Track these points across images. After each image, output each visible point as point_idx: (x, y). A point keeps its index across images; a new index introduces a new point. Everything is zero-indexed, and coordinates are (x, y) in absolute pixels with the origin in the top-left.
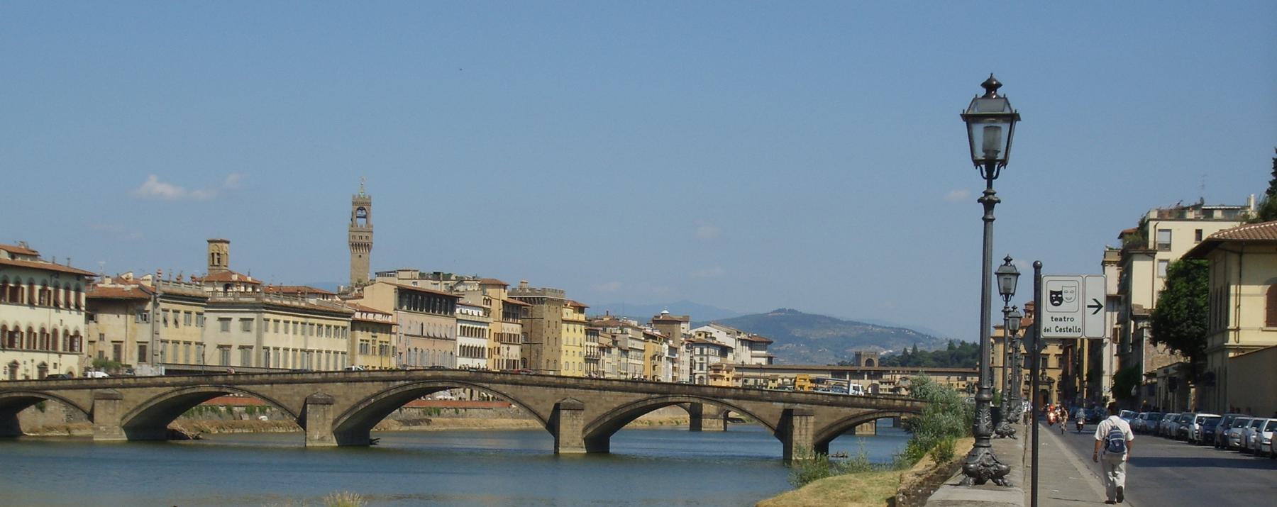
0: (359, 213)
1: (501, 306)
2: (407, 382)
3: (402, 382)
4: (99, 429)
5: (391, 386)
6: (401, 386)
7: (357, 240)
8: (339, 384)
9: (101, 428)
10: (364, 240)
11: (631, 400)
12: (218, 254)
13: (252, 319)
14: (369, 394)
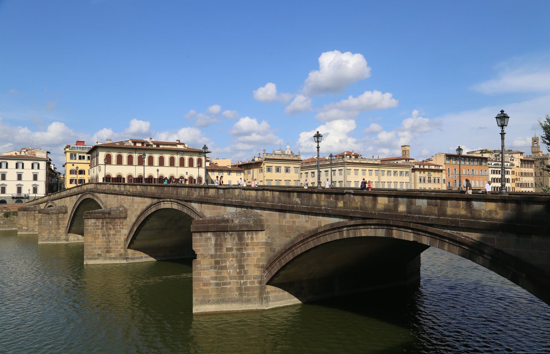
0: (535, 143)
1: (520, 161)
4: (23, 228)
7: (534, 151)
9: (24, 228)
10: (536, 151)
11: (144, 206)
12: (405, 150)
13: (342, 170)
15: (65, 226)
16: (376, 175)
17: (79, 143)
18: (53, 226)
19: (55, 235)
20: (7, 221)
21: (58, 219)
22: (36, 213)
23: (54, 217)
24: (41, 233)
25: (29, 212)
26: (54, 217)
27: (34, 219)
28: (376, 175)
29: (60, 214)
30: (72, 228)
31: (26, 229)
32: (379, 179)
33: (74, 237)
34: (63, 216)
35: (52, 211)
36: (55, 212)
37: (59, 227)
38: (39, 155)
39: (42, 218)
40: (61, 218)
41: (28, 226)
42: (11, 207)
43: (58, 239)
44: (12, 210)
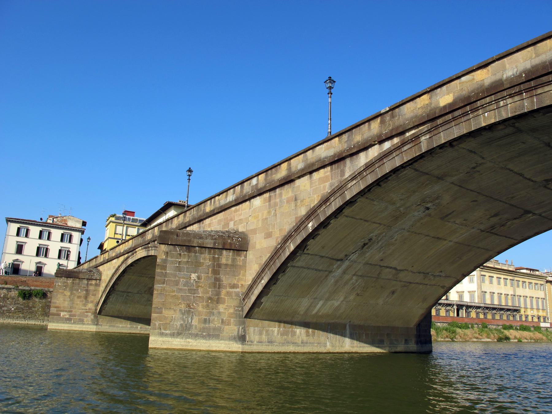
2: (387, 145)
3: (374, 152)
4: (60, 315)
5: (347, 174)
6: (369, 166)
8: (257, 202)
9: (62, 314)
14: (303, 212)
15: (237, 294)
16: (511, 286)
17: (126, 213)
18: (200, 290)
19: (205, 321)
20: (22, 307)
21: (217, 268)
22: (91, 284)
23: (206, 258)
24: (161, 308)
25: (77, 281)
26: (204, 259)
27: (86, 297)
28: (512, 285)
29: (224, 252)
30: (262, 301)
31: (67, 316)
32: (514, 291)
33: (261, 334)
34: (234, 260)
35: (200, 241)
36: (209, 243)
37: (218, 294)
38: (71, 224)
39: (169, 259)
40: (226, 265)
41: (71, 311)
42: (33, 281)
43: (214, 334)
44: (33, 288)
